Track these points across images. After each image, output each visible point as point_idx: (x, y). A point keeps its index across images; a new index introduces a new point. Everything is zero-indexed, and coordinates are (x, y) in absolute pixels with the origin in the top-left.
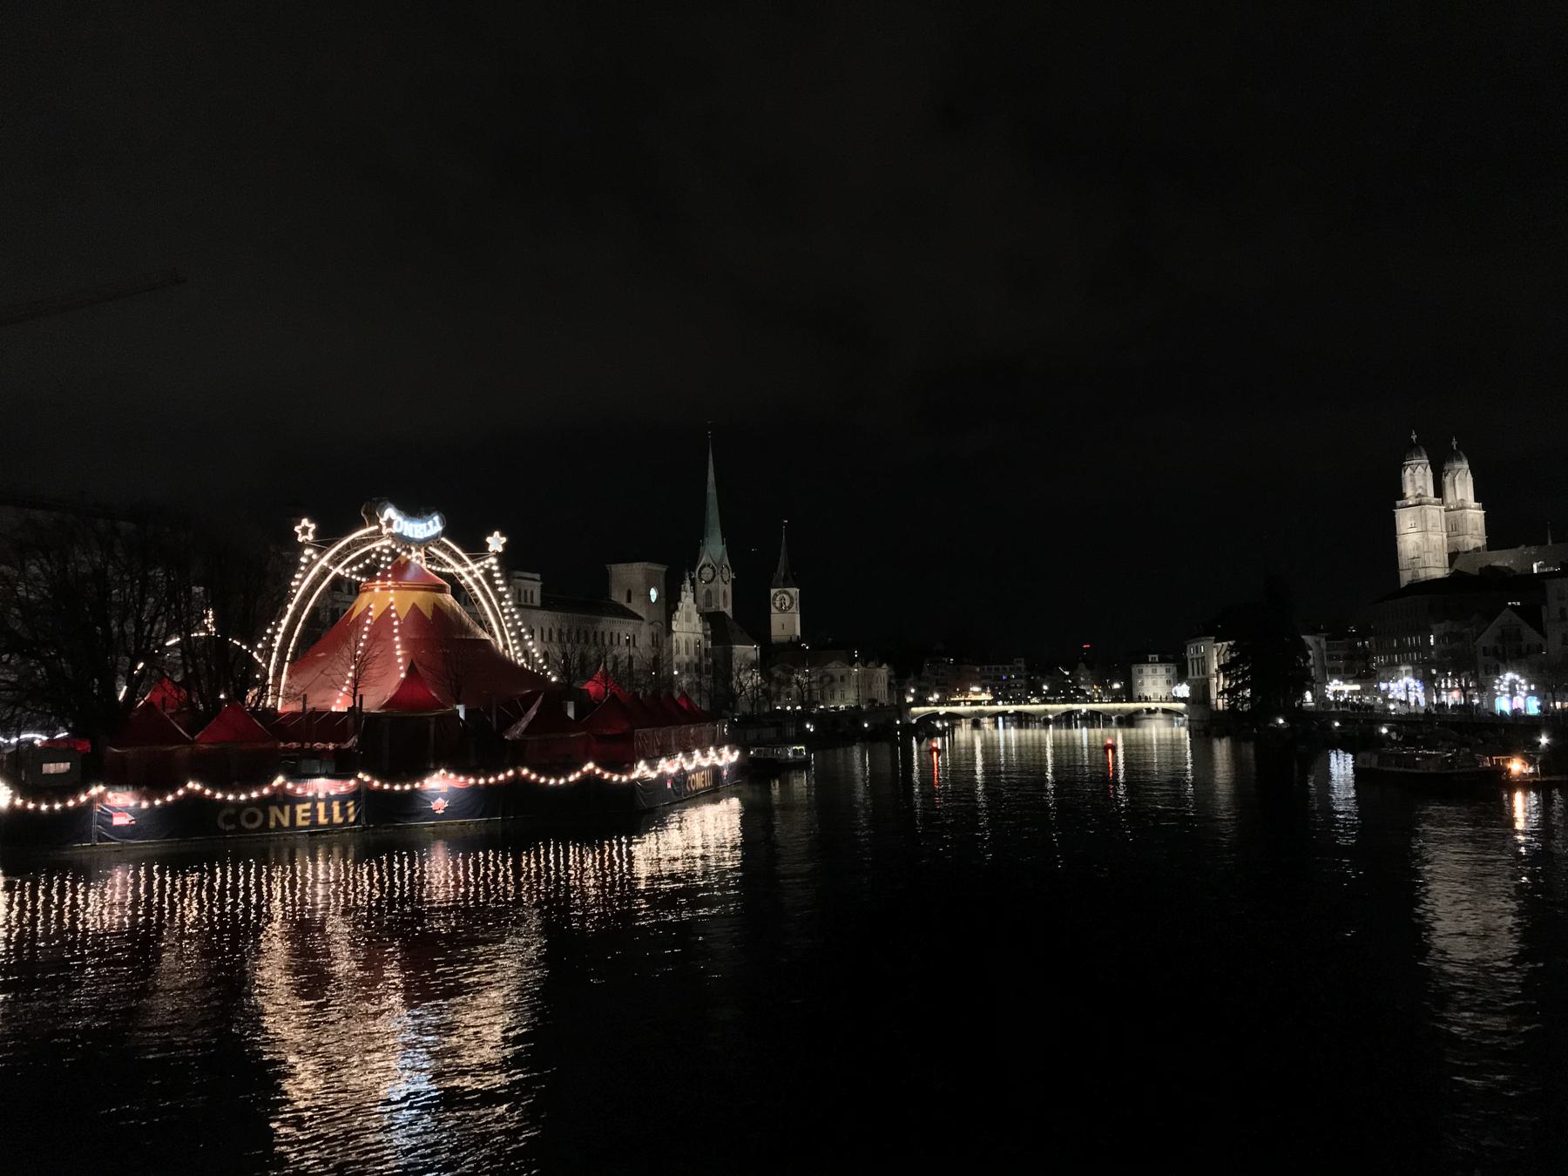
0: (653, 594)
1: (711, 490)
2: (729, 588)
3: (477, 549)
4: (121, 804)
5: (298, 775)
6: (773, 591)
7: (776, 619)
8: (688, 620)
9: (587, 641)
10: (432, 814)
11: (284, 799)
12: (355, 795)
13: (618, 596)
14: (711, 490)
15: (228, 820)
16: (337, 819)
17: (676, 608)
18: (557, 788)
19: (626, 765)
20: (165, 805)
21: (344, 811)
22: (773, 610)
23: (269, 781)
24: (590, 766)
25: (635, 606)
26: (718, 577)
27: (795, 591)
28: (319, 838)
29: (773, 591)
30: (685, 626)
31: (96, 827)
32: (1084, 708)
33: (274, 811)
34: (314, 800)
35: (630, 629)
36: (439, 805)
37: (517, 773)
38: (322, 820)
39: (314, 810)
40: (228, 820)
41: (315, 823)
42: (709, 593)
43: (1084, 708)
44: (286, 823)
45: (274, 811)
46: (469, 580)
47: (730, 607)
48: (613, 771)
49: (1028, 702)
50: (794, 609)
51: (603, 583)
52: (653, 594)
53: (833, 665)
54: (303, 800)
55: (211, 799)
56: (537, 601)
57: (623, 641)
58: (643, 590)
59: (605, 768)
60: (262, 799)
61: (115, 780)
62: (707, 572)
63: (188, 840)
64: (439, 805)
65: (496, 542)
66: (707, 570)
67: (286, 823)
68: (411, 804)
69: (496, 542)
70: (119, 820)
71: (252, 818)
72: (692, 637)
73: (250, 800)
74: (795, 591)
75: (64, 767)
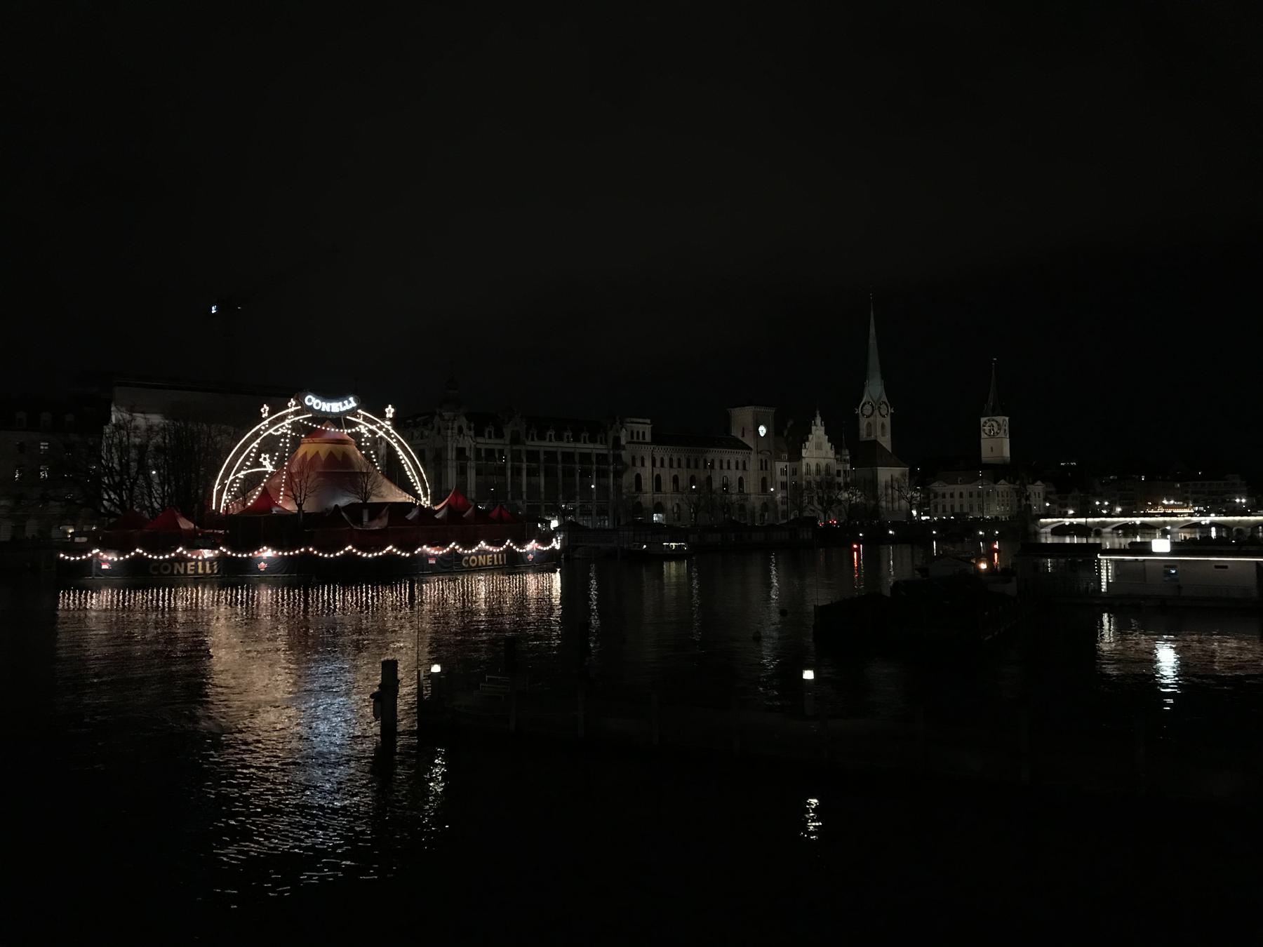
0: (762, 430)
1: (872, 341)
2: (887, 421)
3: (382, 416)
4: (108, 559)
5: (192, 547)
6: (983, 420)
7: (986, 444)
8: (819, 447)
9: (696, 467)
10: (258, 571)
11: (182, 559)
12: (218, 559)
13: (736, 432)
14: (872, 341)
15: (154, 569)
16: (208, 571)
17: (807, 440)
18: (329, 559)
19: (411, 550)
20: (125, 560)
21: (211, 567)
22: (983, 435)
23: (134, 550)
24: (390, 548)
25: (748, 440)
26: (877, 412)
27: (1004, 420)
28: (199, 580)
29: (983, 420)
30: (815, 453)
31: (94, 569)
32: (1138, 520)
33: (177, 565)
34: (197, 560)
35: (740, 458)
36: (262, 565)
37: (307, 550)
38: (200, 571)
39: (196, 566)
40: (154, 569)
41: (196, 573)
42: (869, 425)
43: (1138, 520)
44: (182, 571)
45: (177, 565)
46: (381, 433)
47: (888, 436)
48: (363, 551)
49: (1065, 515)
50: (1002, 434)
51: (727, 423)
52: (762, 430)
53: (936, 484)
54: (191, 560)
55: (146, 558)
56: (648, 438)
57: (733, 466)
58: (751, 427)
59: (359, 549)
60: (171, 559)
61: (105, 548)
62: (868, 407)
63: (137, 576)
64: (262, 565)
65: (390, 411)
66: (868, 407)
67: (182, 571)
68: (250, 565)
69: (390, 411)
70: (105, 567)
71: (166, 568)
72: (823, 463)
73: (165, 560)
74: (1004, 420)
75: (84, 539)
